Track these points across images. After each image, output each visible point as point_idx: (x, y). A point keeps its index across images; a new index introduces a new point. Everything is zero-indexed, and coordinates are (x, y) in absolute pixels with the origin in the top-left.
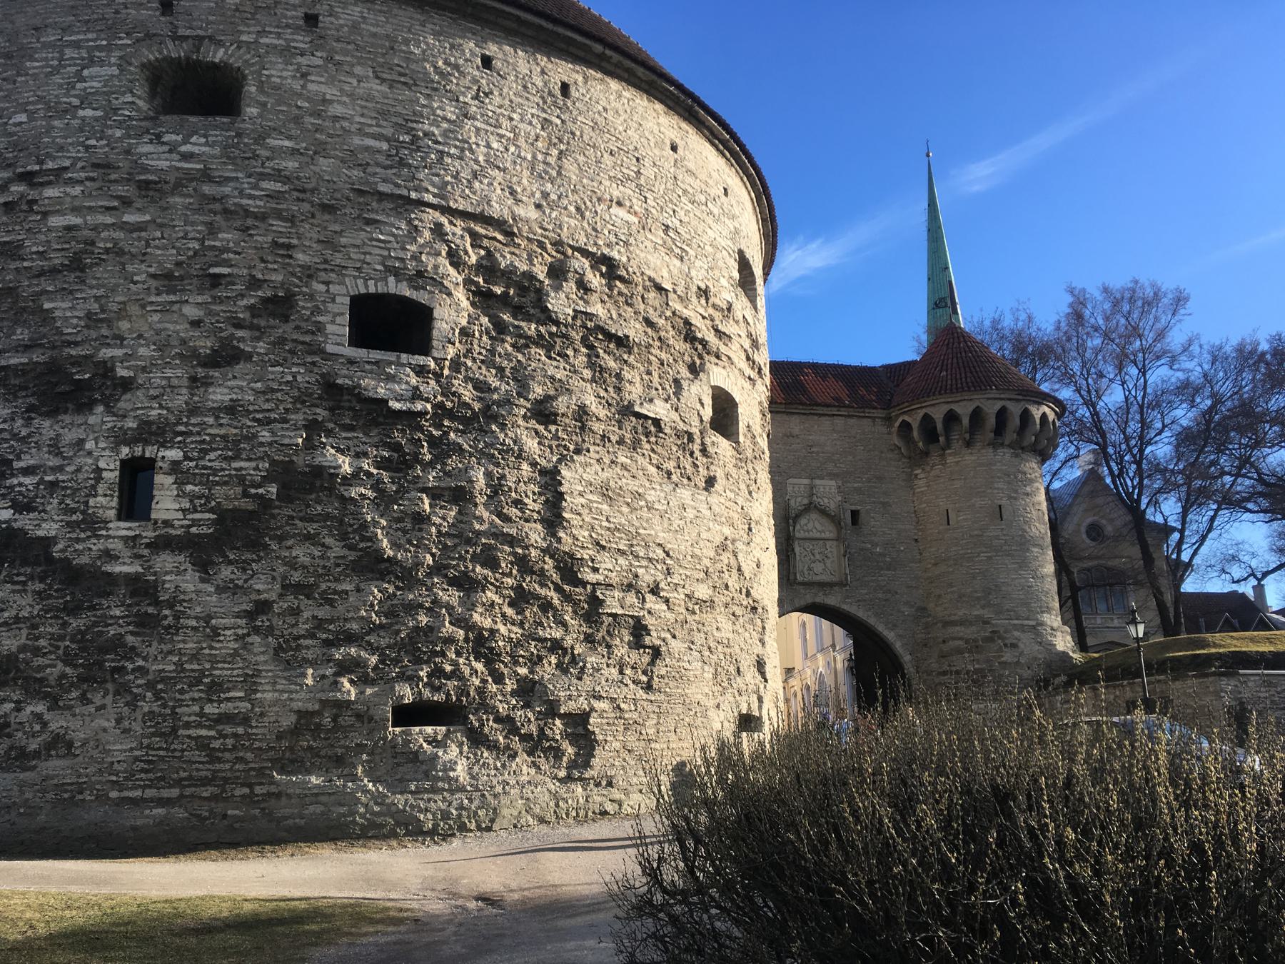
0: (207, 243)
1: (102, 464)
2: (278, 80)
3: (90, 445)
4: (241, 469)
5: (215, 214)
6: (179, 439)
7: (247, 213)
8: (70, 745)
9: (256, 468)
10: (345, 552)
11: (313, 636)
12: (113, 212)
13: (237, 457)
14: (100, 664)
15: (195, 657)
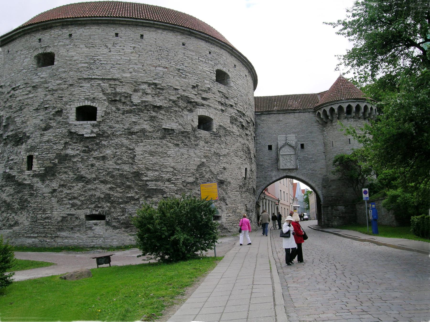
7: (53, 90)
8: (18, 223)
9: (53, 156)
10: (74, 176)
11: (66, 198)
14: (23, 205)
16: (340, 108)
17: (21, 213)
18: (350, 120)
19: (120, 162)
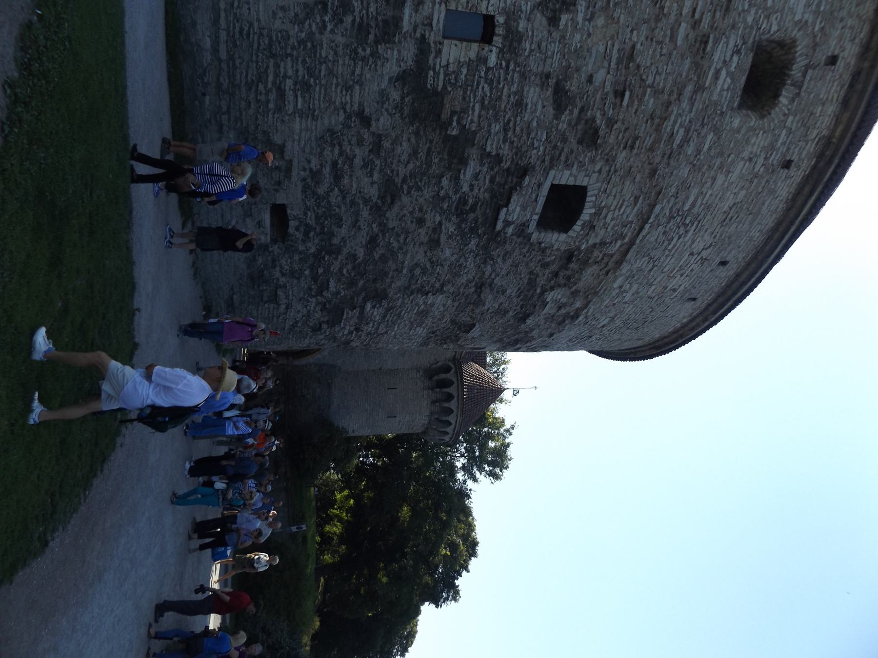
0: (649, 90)
2: (753, 141)
4: (473, 110)
5: (669, 95)
6: (504, 64)
9: (472, 121)
10: (401, 175)
11: (341, 153)
12: (691, 14)
15: (330, 72)
16: (450, 411)
18: (427, 418)
19: (418, 271)
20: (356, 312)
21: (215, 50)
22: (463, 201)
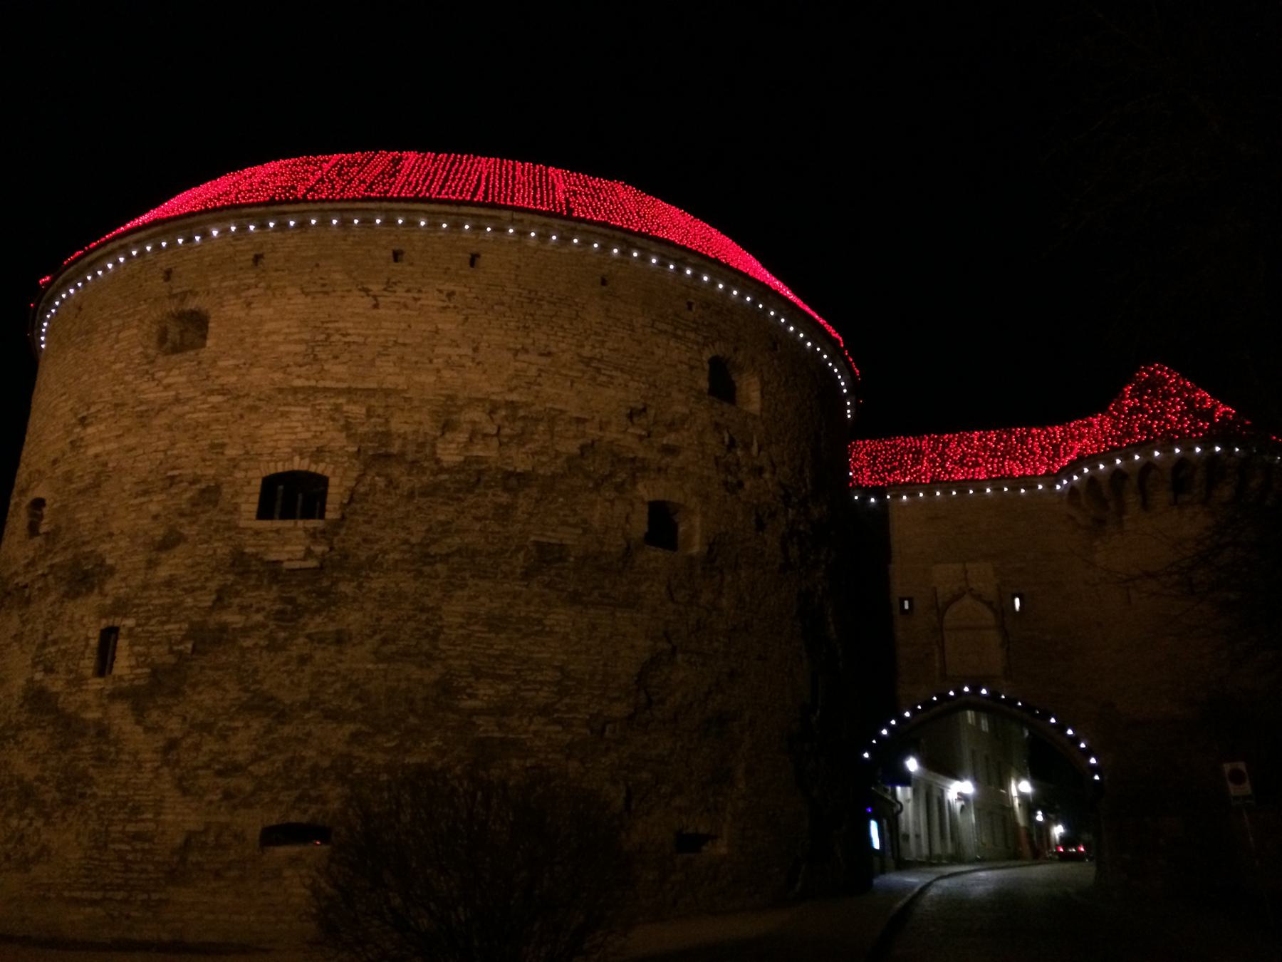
1: (90, 634)
3: (86, 620)
7: (198, 424)
9: (180, 629)
11: (208, 767)
13: (167, 622)
17: (64, 818)
19: (389, 649)
20: (479, 721)
21: (93, 903)
22: (280, 616)
